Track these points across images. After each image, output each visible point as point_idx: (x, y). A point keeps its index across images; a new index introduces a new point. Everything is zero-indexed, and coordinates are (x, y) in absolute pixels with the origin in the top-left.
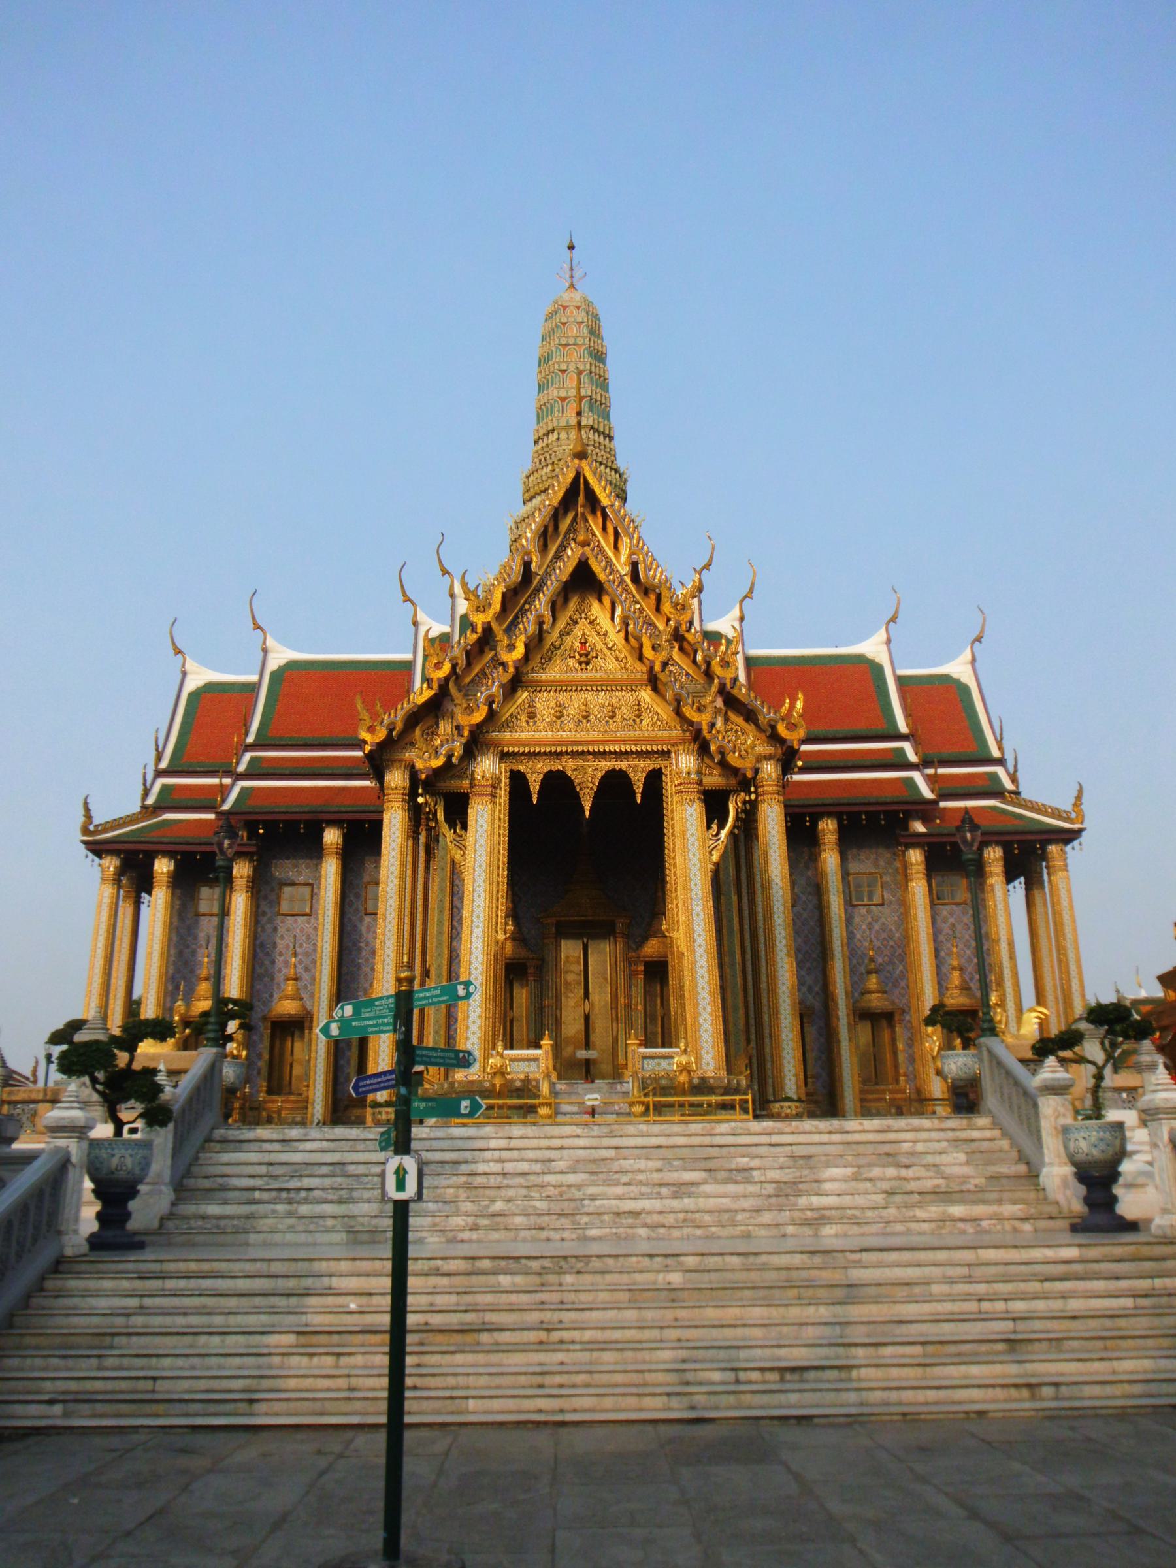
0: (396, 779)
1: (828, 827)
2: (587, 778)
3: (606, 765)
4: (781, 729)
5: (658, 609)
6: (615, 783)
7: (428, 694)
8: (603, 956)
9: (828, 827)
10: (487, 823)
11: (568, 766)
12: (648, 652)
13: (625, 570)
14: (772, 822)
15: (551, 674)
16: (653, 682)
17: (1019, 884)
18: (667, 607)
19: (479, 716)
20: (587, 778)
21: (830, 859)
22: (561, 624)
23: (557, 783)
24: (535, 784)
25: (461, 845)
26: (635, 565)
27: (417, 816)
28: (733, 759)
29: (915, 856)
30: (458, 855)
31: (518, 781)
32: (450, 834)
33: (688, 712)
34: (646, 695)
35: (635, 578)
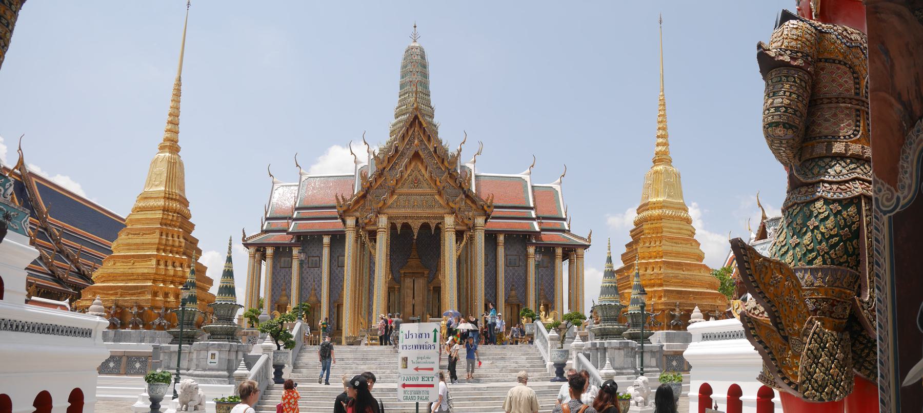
0: (351, 222)
1: (501, 238)
2: (416, 225)
3: (422, 221)
4: (485, 207)
5: (443, 162)
6: (425, 227)
7: (362, 193)
8: (420, 283)
9: (501, 238)
10: (382, 240)
11: (410, 222)
12: (438, 183)
13: (432, 150)
14: (480, 238)
15: (404, 190)
16: (440, 193)
17: (567, 261)
18: (446, 163)
19: (380, 205)
20: (416, 225)
21: (501, 251)
22: (409, 172)
23: (406, 226)
24: (399, 226)
25: (374, 248)
26: (435, 148)
27: (358, 236)
28: (466, 221)
29: (531, 250)
30: (373, 251)
31: (393, 227)
32: (370, 245)
33: (451, 204)
34: (437, 197)
35: (435, 151)
